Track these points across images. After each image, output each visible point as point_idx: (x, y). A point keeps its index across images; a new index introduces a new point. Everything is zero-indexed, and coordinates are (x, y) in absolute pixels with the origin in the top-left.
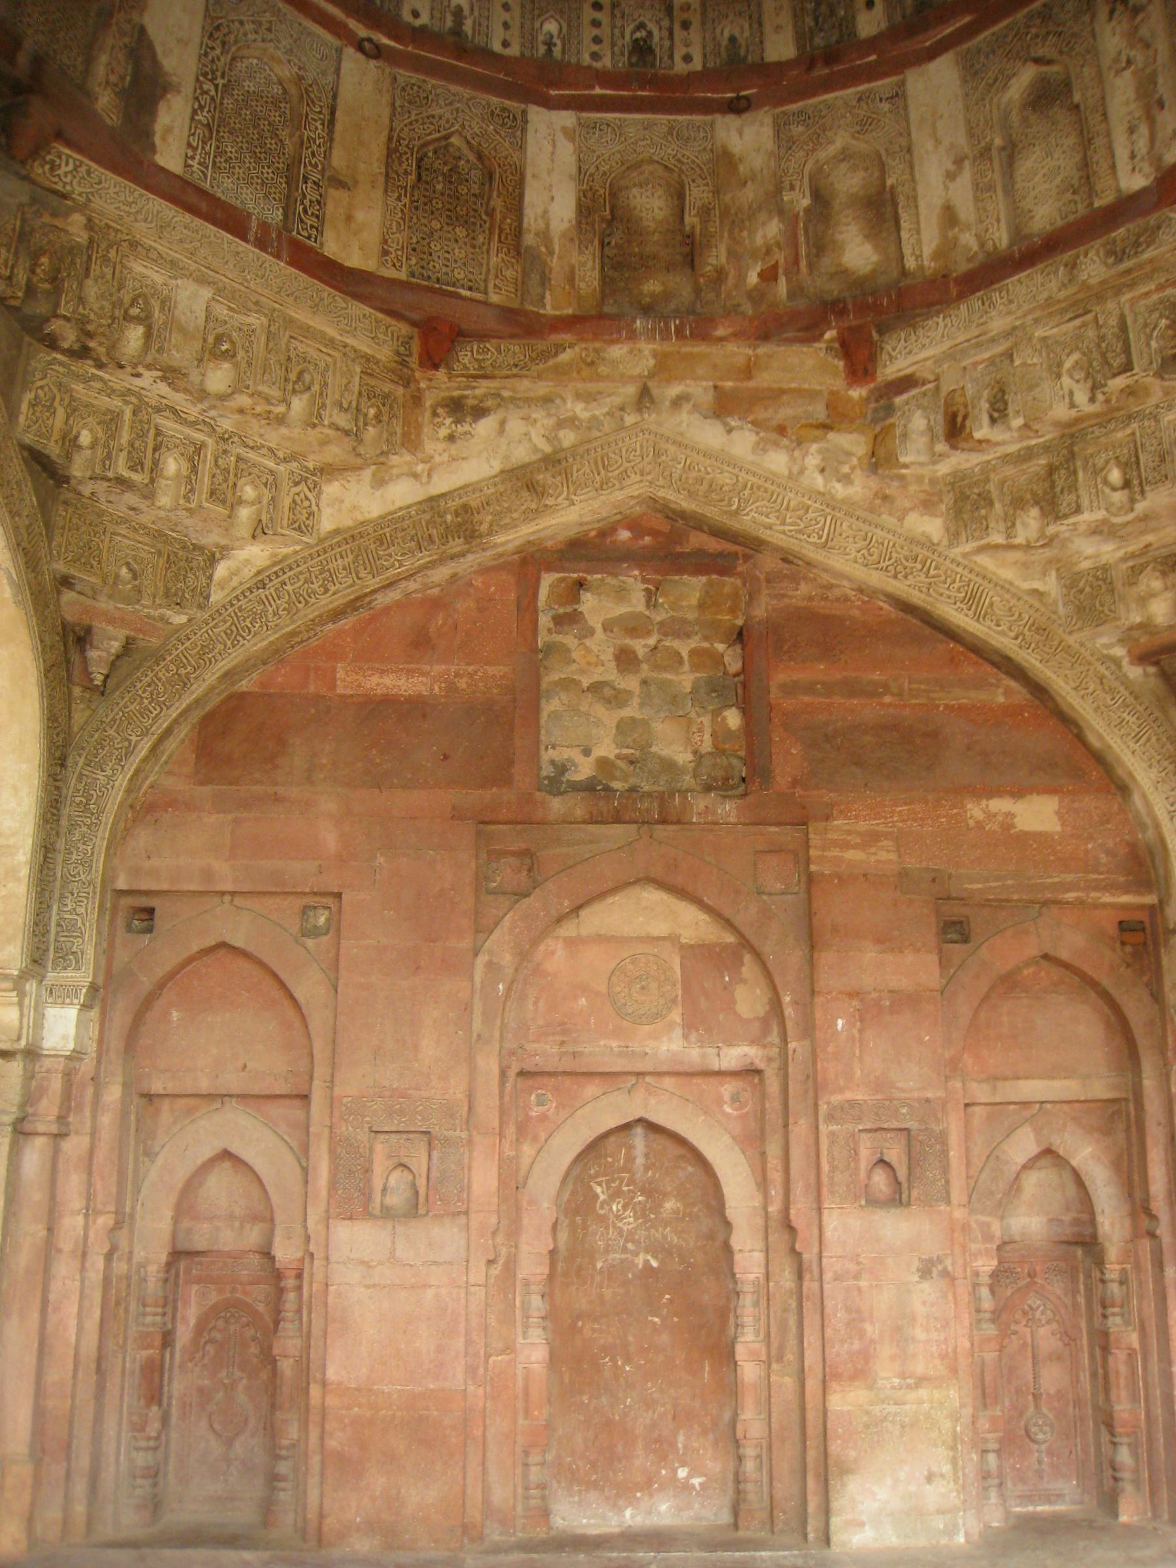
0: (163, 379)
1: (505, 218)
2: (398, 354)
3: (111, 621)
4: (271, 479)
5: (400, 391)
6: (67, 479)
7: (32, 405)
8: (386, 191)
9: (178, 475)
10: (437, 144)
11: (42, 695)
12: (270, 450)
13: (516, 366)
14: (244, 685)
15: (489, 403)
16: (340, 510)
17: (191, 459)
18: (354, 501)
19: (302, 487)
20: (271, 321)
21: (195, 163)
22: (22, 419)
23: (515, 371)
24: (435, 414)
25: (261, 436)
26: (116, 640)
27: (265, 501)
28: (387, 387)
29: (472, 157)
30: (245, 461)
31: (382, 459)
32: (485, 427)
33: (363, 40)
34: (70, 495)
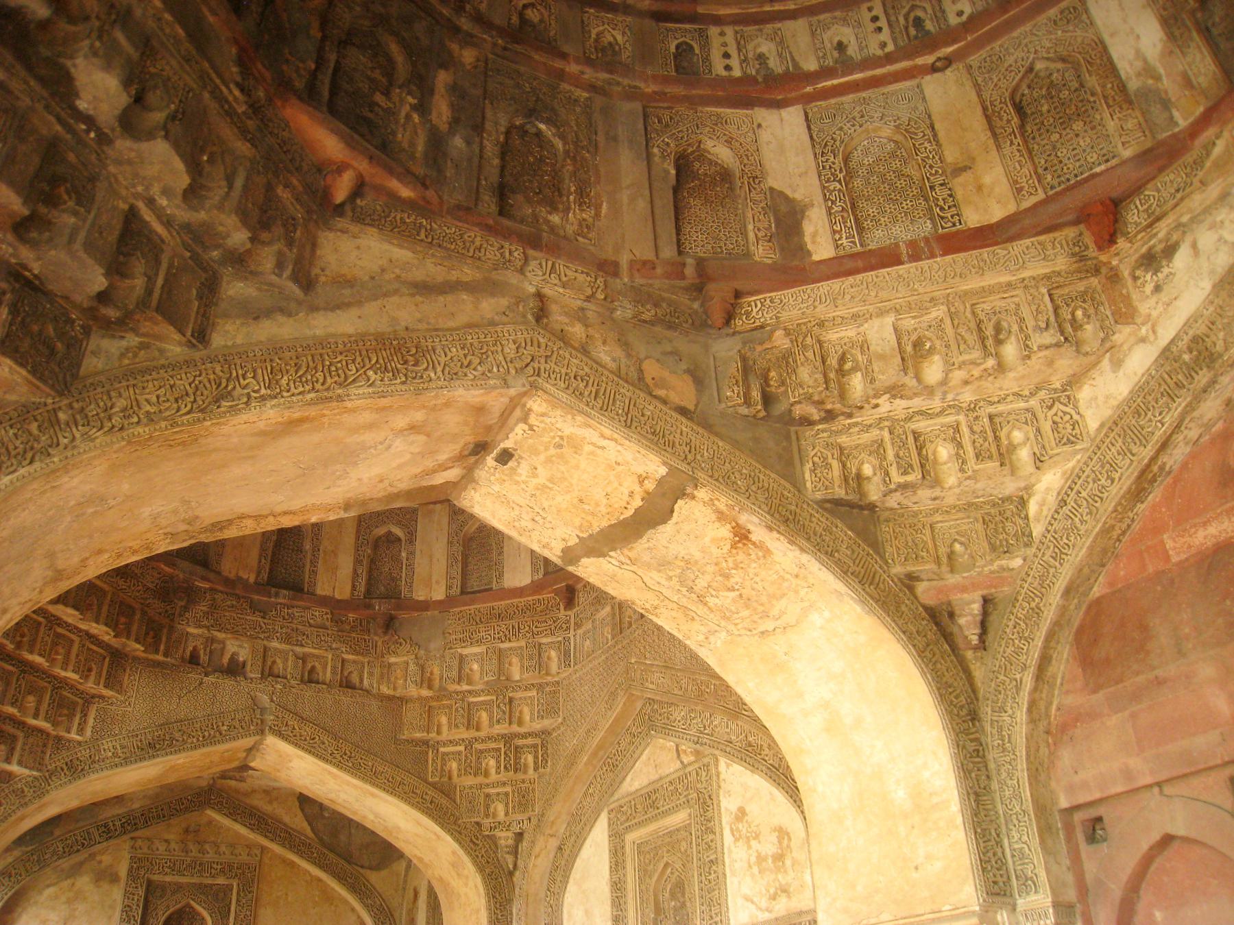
0: (894, 397)
1: (1104, 87)
2: (1074, 255)
3: (964, 589)
4: (1029, 416)
5: (1094, 281)
6: (872, 507)
7: (813, 471)
8: (999, 147)
9: (950, 457)
10: (1026, 81)
11: (923, 673)
12: (1016, 394)
13: (1178, 191)
14: (1097, 591)
15: (1175, 237)
16: (1098, 406)
17: (954, 439)
18: (1105, 392)
19: (1057, 406)
20: (949, 304)
21: (844, 241)
22: (809, 485)
23: (1179, 196)
24: (1135, 278)
25: (1001, 389)
26: (974, 602)
27: (1032, 436)
28: (1081, 286)
29: (1060, 65)
30: (1000, 415)
31: (1108, 345)
32: (1182, 258)
33: (933, 64)
34: (887, 513)
